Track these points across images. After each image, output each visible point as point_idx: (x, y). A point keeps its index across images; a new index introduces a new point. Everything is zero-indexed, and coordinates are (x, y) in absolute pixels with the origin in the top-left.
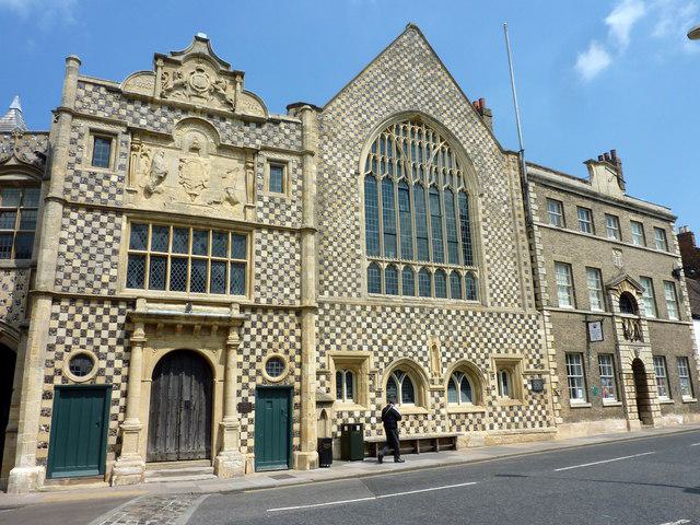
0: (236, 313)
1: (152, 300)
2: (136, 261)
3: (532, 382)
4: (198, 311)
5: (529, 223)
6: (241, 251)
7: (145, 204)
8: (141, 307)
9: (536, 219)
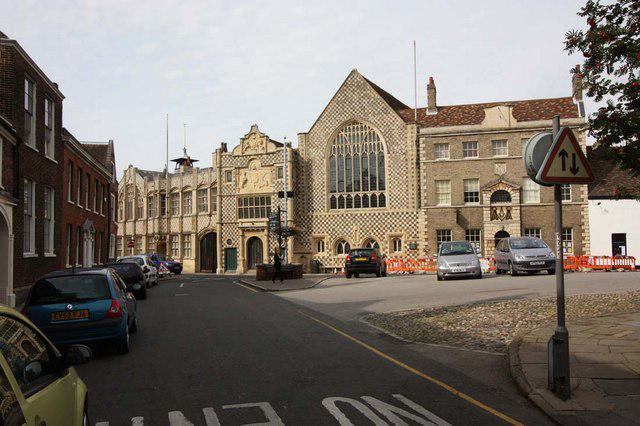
0: (265, 224)
1: (247, 222)
2: (240, 210)
3: (410, 245)
4: (257, 225)
5: (418, 164)
6: (269, 202)
7: (243, 192)
8: (240, 225)
9: (423, 159)
